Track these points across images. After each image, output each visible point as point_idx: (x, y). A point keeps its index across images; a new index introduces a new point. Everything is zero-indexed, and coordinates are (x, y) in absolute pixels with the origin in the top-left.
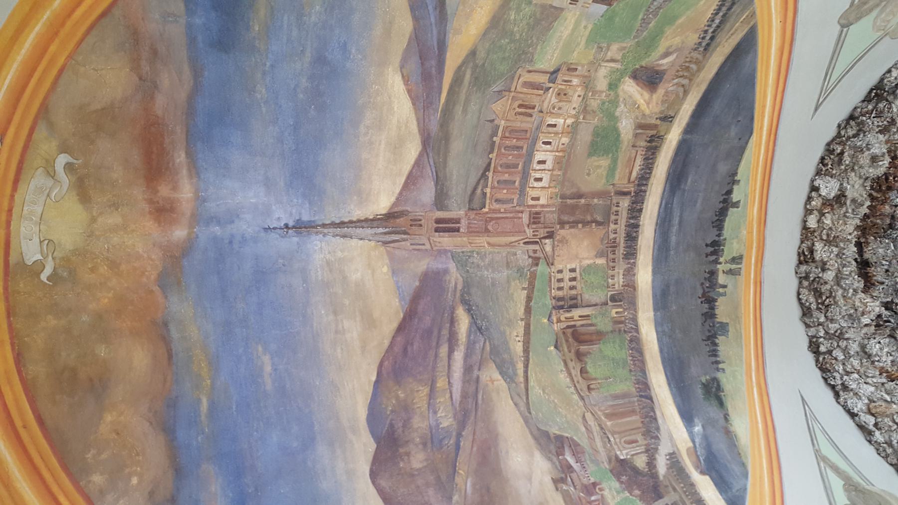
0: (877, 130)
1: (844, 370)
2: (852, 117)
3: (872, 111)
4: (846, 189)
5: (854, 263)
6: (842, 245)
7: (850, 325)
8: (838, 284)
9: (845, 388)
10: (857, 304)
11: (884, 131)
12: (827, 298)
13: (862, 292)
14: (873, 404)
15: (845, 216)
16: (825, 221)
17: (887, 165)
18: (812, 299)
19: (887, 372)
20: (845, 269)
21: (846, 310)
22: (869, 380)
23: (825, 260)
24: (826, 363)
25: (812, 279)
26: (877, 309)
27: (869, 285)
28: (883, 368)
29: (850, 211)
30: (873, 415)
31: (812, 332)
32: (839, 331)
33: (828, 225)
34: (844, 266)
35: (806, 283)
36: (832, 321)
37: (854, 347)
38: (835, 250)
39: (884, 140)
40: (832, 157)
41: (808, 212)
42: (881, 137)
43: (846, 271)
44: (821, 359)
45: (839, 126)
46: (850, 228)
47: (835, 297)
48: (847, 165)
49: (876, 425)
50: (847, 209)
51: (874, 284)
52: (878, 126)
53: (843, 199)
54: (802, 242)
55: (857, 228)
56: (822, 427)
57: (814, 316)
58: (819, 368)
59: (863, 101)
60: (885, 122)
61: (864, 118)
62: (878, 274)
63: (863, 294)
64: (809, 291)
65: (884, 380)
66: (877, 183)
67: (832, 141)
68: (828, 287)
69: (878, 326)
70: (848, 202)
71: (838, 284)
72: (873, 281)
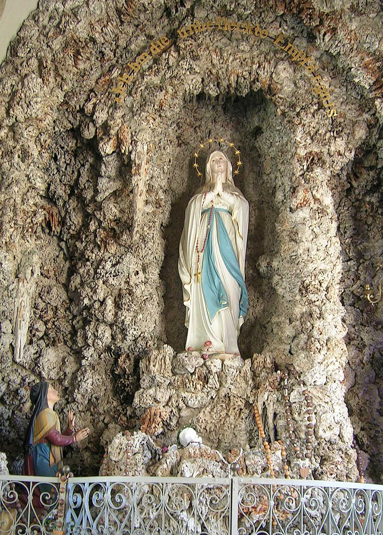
0: (355, 3)
39: (345, 8)
42: (348, 6)
60: (361, 8)
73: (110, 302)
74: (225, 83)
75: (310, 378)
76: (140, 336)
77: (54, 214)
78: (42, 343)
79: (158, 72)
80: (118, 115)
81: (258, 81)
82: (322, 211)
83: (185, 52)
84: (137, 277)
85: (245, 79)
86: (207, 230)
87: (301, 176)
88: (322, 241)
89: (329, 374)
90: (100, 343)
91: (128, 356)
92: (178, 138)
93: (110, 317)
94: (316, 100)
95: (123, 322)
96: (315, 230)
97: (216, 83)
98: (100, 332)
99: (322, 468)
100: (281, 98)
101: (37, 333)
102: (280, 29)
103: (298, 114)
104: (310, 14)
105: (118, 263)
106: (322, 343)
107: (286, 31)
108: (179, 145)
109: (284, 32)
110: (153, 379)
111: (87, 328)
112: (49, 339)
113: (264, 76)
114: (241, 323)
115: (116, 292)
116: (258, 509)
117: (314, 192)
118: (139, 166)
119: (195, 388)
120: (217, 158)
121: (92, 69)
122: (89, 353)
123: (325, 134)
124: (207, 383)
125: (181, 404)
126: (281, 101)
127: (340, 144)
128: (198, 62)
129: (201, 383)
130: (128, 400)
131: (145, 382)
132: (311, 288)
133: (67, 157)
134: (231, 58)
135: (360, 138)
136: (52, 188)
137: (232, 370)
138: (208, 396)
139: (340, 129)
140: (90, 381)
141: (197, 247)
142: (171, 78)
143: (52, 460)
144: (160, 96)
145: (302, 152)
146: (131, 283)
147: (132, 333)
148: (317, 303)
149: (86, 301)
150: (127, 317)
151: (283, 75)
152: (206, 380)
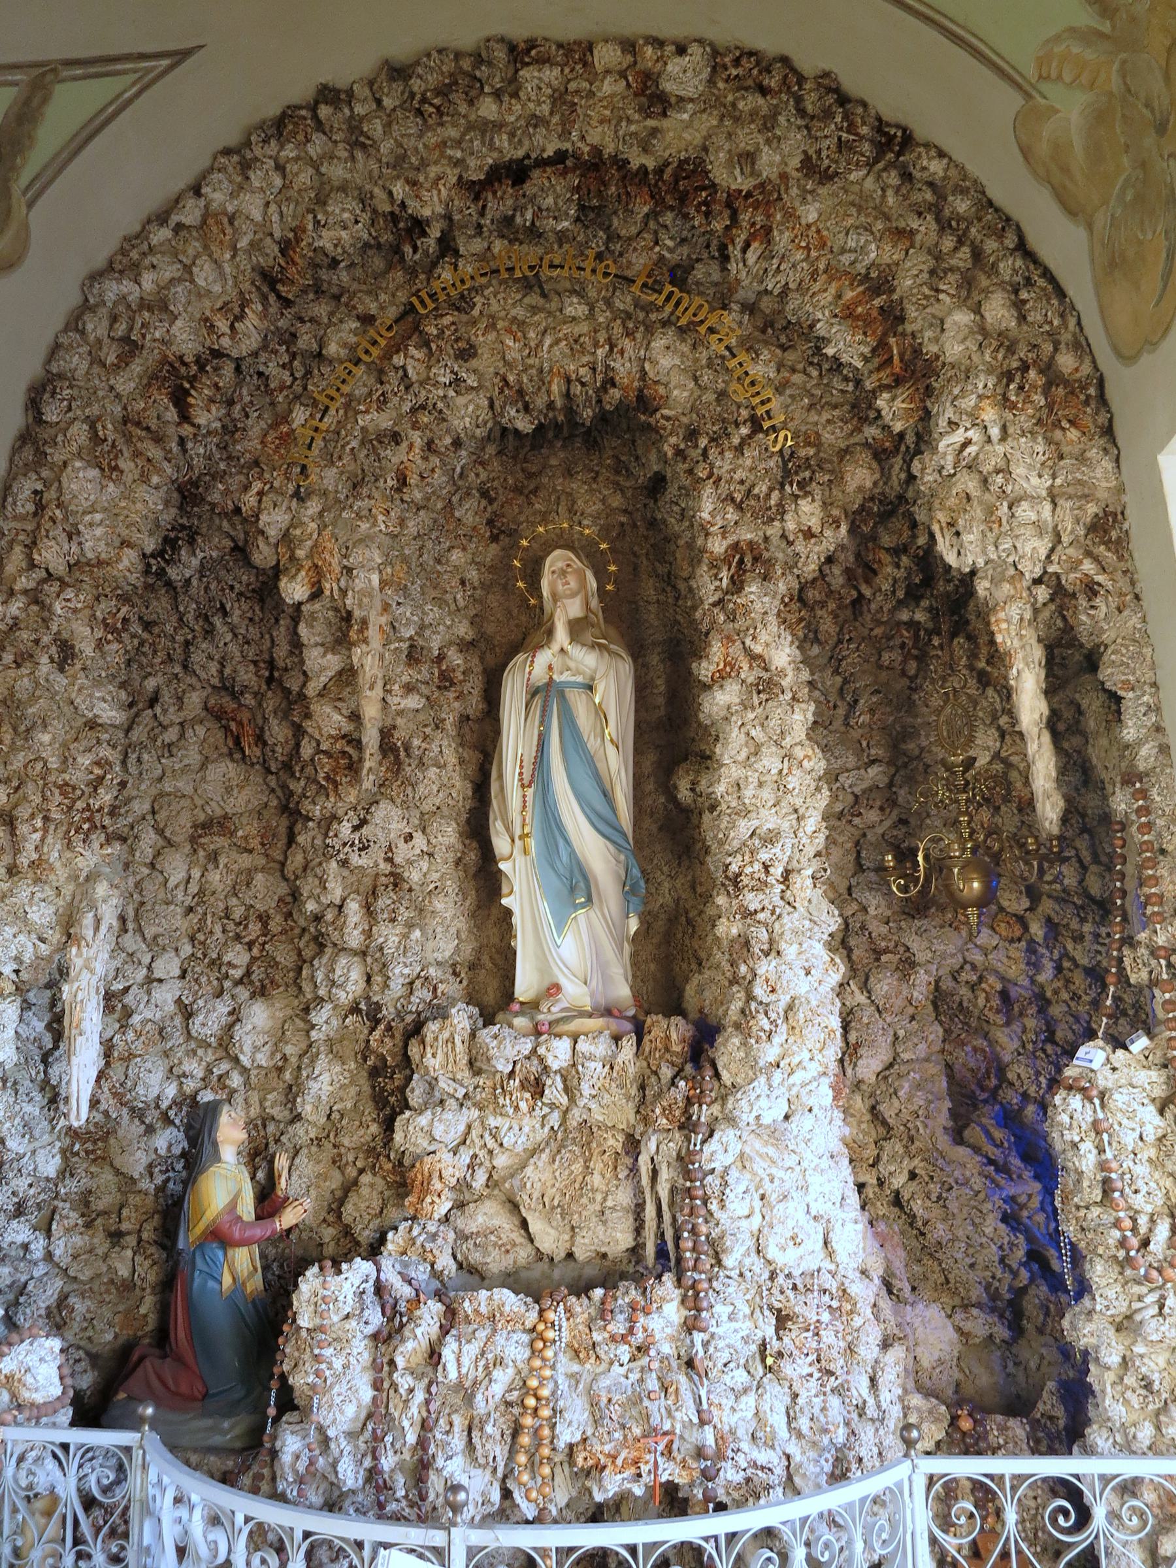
0: (811, 152)
1: (288, 160)
2: (843, 100)
3: (857, 134)
4: (682, 110)
5: (520, 153)
6: (556, 119)
7: (384, 160)
8: (470, 127)
9: (246, 166)
10: (433, 171)
11: (809, 166)
12: (438, 108)
13: (460, 177)
14: (225, 221)
15: (620, 119)
16: (606, 82)
17: (733, 187)
18: (433, 79)
19: (298, 240)
20: (505, 137)
21: (416, 149)
22: (273, 207)
23: (521, 94)
24: (296, 124)
25: (478, 73)
26: (427, 212)
27: (476, 190)
28: (304, 231)
29: (633, 128)
30: (204, 222)
31: (361, 91)
32: (368, 142)
33: (600, 90)
34: (512, 135)
35: (466, 64)
36: (388, 126)
37: (337, 172)
38: (546, 108)
39: (788, 170)
40: (755, 72)
41: (629, 46)
42: (795, 162)
43: (502, 140)
44: (303, 112)
45: (826, 74)
46: (594, 137)
47: (442, 124)
48: (734, 105)
49: (179, 227)
50: (638, 122)
51: (477, 198)
52: (819, 152)
53: (657, 109)
54: (560, 46)
55: (597, 151)
56: (130, 101)
57: (394, 85)
58: (284, 112)
59: (879, 119)
60: (826, 162)
61: (838, 119)
62: (499, 204)
63: (454, 180)
64: (451, 75)
65: (277, 234)
66: (693, 171)
67: (793, 70)
68: (463, 108)
69: (394, 218)
70: (651, 123)
71: (470, 127)
72: (483, 196)
73: (353, 907)
74: (540, 402)
75: (746, 1109)
76: (418, 977)
77: (245, 721)
78: (243, 993)
79: (385, 402)
80: (310, 512)
81: (614, 385)
82: (766, 687)
83: (440, 343)
84: (411, 844)
85: (583, 384)
86: (540, 735)
87: (714, 605)
88: (770, 762)
89: (794, 1091)
90: (343, 995)
91: (389, 1028)
92: (490, 523)
93: (354, 939)
94: (745, 413)
95: (381, 949)
96: (753, 733)
97: (520, 405)
98: (338, 972)
99: (779, 1339)
100: (668, 419)
101: (231, 972)
102: (657, 249)
103: (705, 453)
104: (706, 203)
105: (363, 822)
106: (773, 1016)
107: (670, 250)
108: (494, 538)
109: (667, 255)
110: (432, 1084)
111: (316, 962)
112: (251, 983)
113: (623, 369)
114: (633, 925)
115: (368, 881)
116: (619, 1462)
117: (748, 642)
118: (364, 623)
119: (517, 1108)
120: (560, 564)
121: (247, 416)
122: (320, 1016)
123: (768, 496)
124: (542, 1094)
125: (491, 1143)
126: (668, 425)
127: (809, 512)
128: (474, 363)
129: (528, 1095)
130: (389, 1127)
131: (416, 1095)
132: (745, 880)
133: (245, 607)
134: (548, 341)
135: (860, 489)
136: (227, 671)
137: (592, 1065)
138: (543, 1126)
139: (807, 474)
140: (325, 1078)
141: (521, 774)
142: (414, 410)
143: (227, 1280)
144: (395, 456)
145: (718, 546)
146: (398, 860)
147: (399, 973)
148: (761, 916)
149: (311, 906)
150: (389, 936)
151: (666, 362)
152: (537, 1088)
